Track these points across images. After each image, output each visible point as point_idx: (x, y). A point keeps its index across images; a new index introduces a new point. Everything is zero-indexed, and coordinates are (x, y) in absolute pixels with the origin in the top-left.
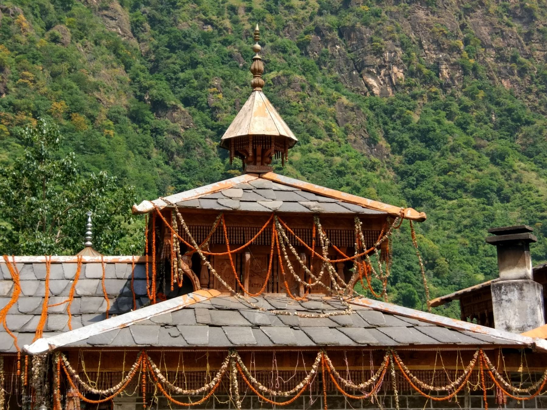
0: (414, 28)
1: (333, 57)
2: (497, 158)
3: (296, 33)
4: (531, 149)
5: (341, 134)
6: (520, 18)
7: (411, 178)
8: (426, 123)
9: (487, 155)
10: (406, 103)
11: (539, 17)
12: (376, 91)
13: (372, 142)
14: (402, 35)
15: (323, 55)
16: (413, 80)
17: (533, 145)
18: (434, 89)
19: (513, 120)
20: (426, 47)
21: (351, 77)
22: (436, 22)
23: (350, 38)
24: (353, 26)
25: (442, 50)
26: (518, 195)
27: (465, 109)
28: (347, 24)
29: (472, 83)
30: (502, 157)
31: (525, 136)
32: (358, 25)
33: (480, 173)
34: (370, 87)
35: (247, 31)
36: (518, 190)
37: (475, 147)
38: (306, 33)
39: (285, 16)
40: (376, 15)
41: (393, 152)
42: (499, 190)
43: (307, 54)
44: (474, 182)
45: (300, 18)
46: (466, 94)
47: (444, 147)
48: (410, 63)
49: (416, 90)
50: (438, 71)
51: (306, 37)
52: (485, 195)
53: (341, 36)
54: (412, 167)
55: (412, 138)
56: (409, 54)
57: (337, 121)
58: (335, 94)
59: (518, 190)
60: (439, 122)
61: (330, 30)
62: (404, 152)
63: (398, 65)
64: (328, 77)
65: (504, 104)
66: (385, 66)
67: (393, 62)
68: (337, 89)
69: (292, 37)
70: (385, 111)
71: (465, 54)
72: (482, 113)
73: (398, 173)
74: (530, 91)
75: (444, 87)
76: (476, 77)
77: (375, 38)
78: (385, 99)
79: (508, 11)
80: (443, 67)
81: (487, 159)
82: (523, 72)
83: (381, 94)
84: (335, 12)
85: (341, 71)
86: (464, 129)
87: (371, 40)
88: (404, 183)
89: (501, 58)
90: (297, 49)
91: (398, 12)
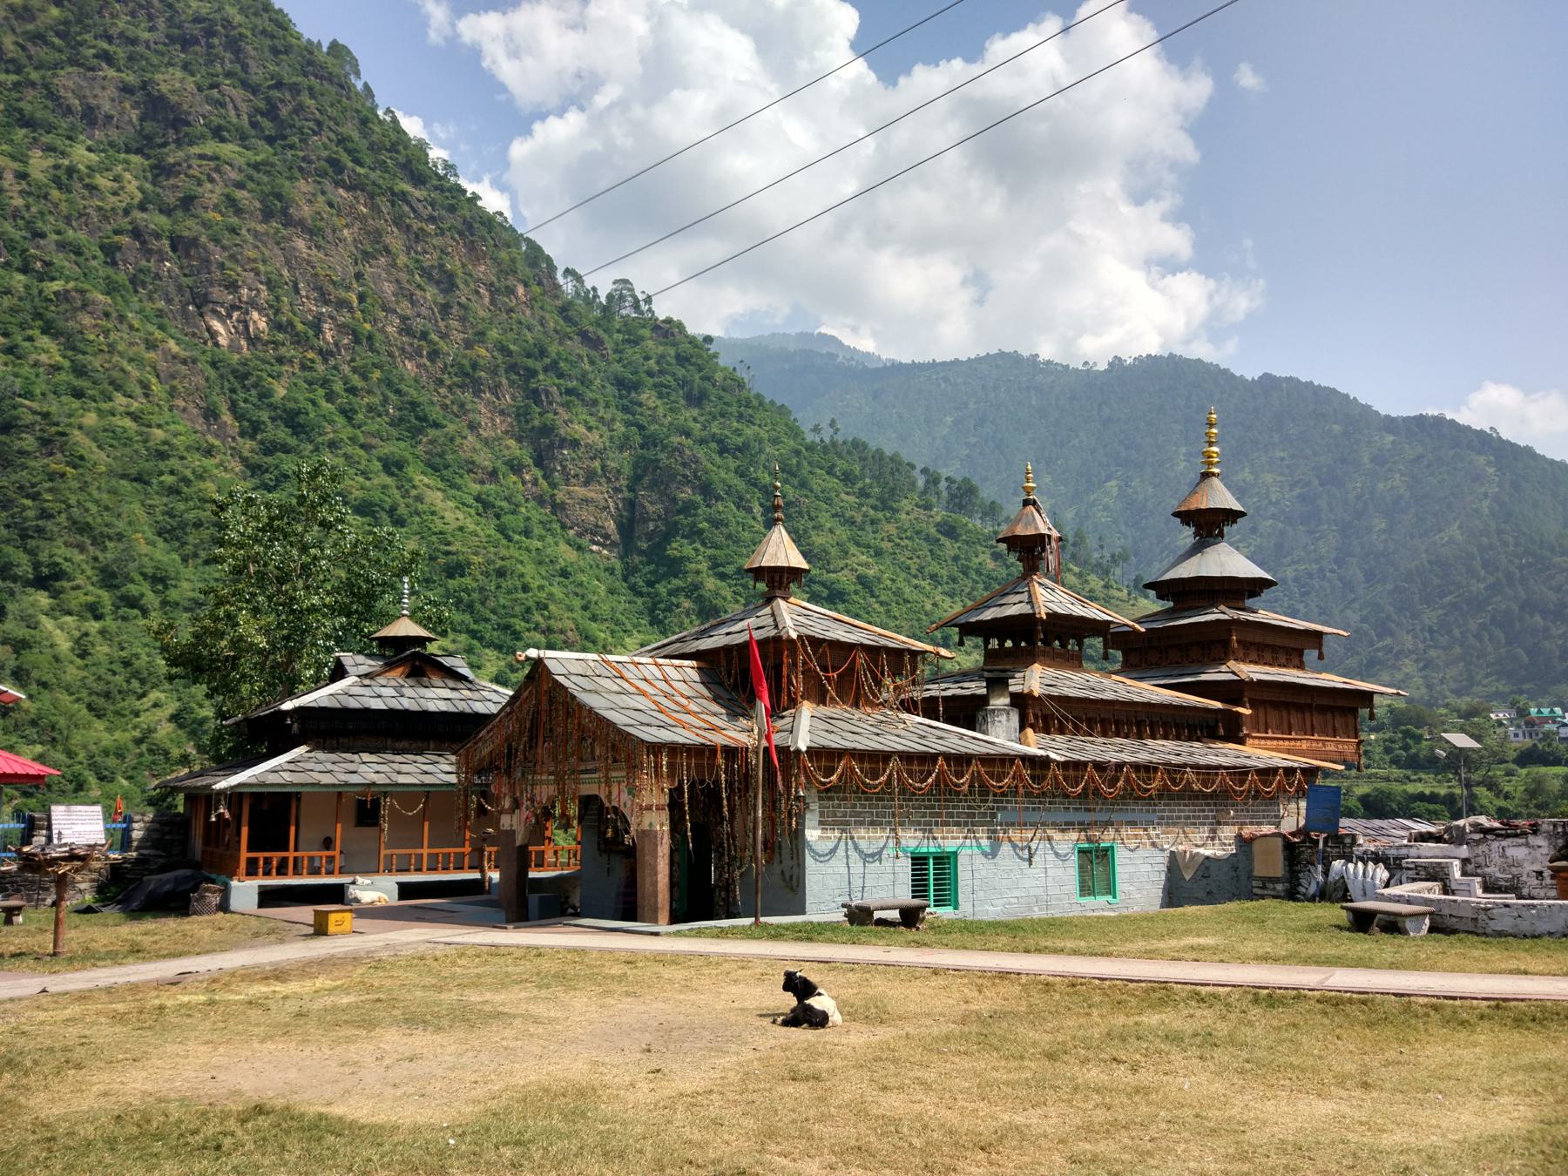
0: (288, 262)
1: (158, 276)
2: (392, 466)
3: (99, 229)
4: (437, 460)
5: (164, 395)
6: (438, 283)
7: (267, 476)
8: (296, 401)
9: (379, 459)
10: (268, 367)
11: (461, 286)
12: (223, 341)
13: (210, 414)
14: (269, 269)
15: (141, 271)
16: (280, 337)
17: (442, 455)
18: (310, 355)
19: (417, 418)
20: (303, 293)
21: (185, 313)
22: (322, 261)
23: (188, 256)
24: (195, 239)
25: (327, 303)
26: (417, 519)
27: (352, 391)
28: (186, 233)
29: (365, 356)
30: (400, 465)
31: (431, 442)
32: (203, 239)
33: (368, 483)
34: (213, 334)
35: (17, 209)
36: (418, 514)
37: (362, 446)
38: (117, 232)
39: (84, 198)
40: (234, 231)
41: (242, 434)
42: (392, 511)
43: (114, 264)
44: (357, 493)
45: (108, 207)
46: (354, 370)
47: (320, 439)
48: (277, 312)
49: (283, 351)
51: (116, 238)
52: (372, 514)
53: (174, 248)
54: (269, 460)
55: (273, 419)
56: (278, 299)
57: (158, 376)
58: (158, 334)
59: (418, 514)
60: (314, 403)
61: (158, 236)
62: (259, 437)
63: (260, 310)
64: (149, 305)
65: (406, 394)
66: (238, 308)
67: (253, 304)
68: (161, 327)
69: (91, 233)
70: (234, 372)
71: (359, 314)
72: (376, 400)
73: (247, 466)
74: (440, 382)
75: (325, 355)
76: (372, 349)
77: (228, 264)
78: (237, 356)
79: (422, 269)
80: (326, 326)
81: (378, 465)
82: (434, 355)
83: (230, 346)
84: (167, 211)
85: (169, 301)
86: (350, 419)
87: (222, 266)
88: (256, 481)
89: (406, 330)
90: (99, 253)
91: (267, 234)
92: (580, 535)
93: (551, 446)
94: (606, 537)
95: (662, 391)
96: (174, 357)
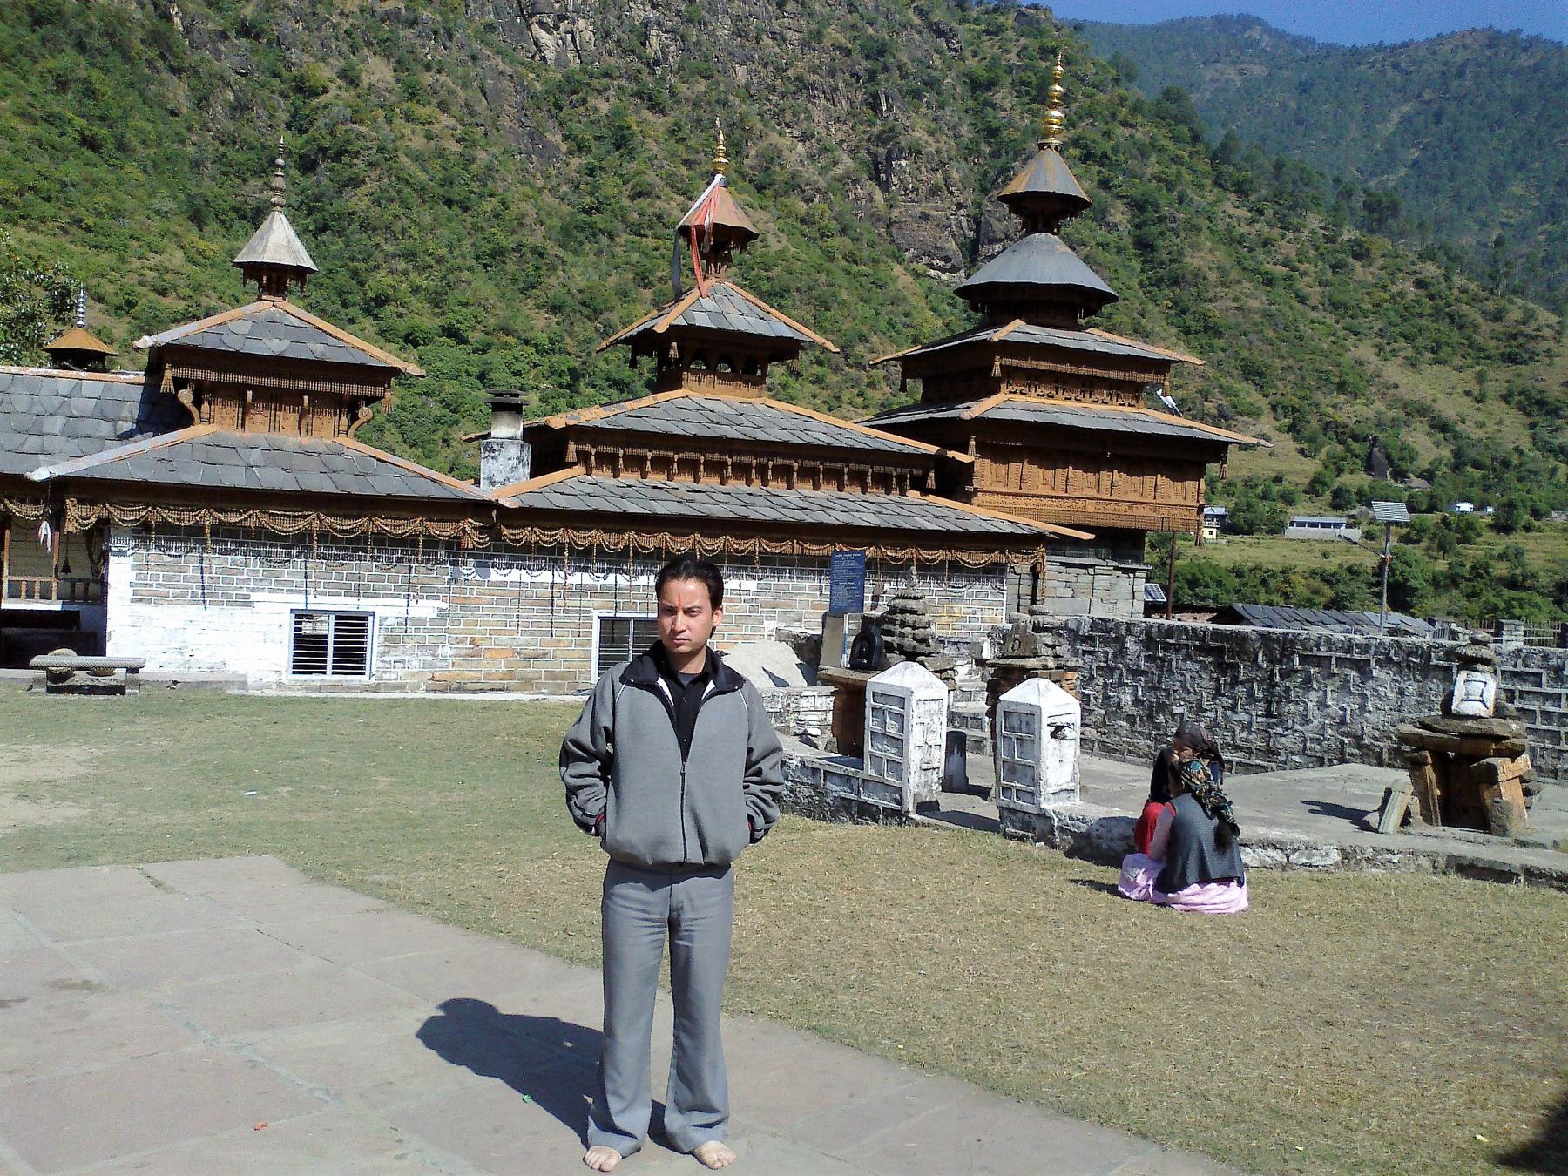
50: (644, 40)
74: (772, 89)
92: (917, 258)
93: (889, 159)
94: (947, 259)
95: (1020, 87)
96: (502, 73)
